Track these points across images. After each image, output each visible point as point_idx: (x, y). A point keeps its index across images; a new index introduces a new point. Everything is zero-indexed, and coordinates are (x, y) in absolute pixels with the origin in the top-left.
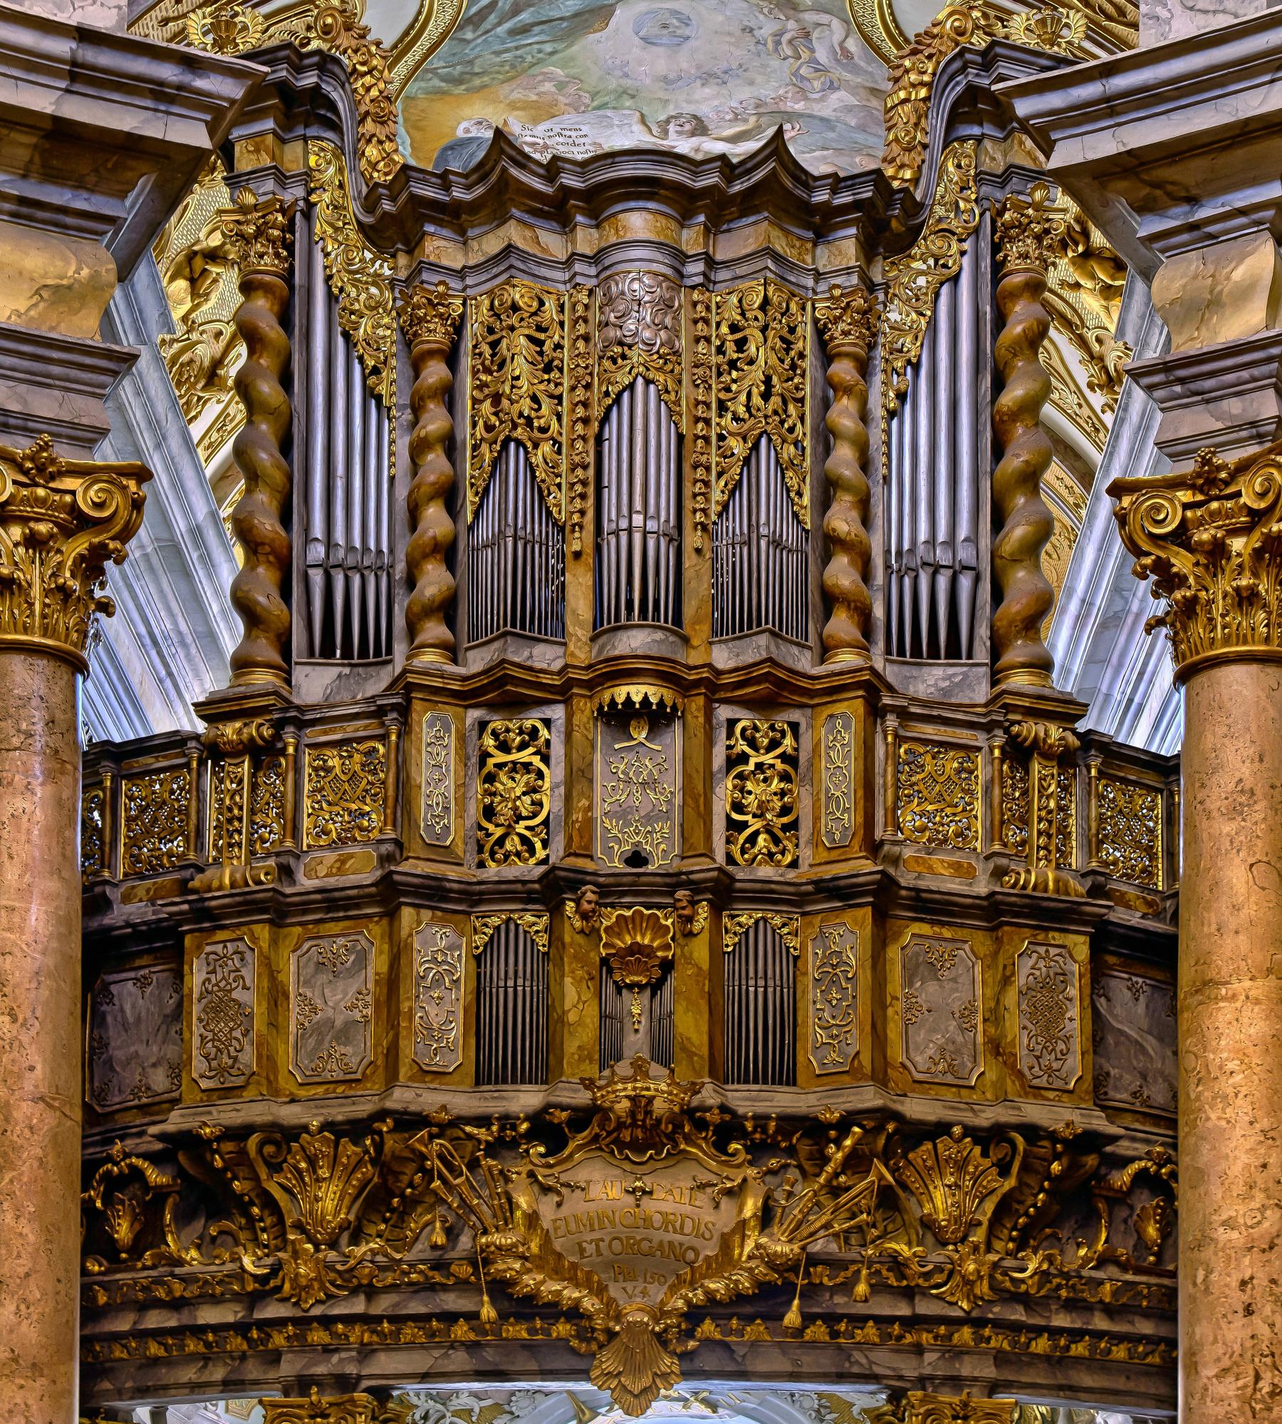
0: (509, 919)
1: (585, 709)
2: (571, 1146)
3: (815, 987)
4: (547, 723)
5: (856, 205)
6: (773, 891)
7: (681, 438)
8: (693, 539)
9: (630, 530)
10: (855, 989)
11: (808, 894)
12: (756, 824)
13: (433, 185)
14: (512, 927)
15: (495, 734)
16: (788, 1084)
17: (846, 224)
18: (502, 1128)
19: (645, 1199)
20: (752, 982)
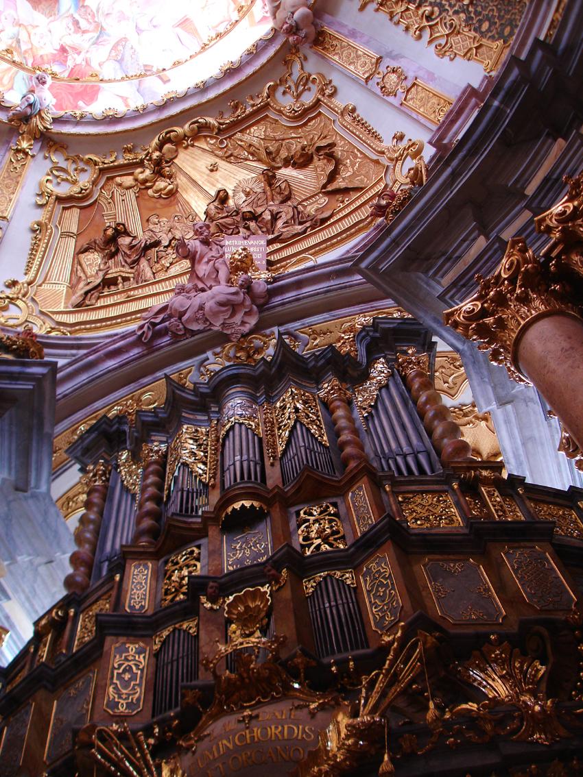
0: (175, 629)
1: (213, 531)
2: (204, 719)
3: (369, 596)
4: (199, 547)
5: (328, 362)
6: (330, 558)
7: (260, 440)
8: (267, 463)
9: (234, 464)
10: (391, 580)
11: (353, 554)
12: (319, 541)
13: (151, 416)
14: (177, 632)
15: (172, 561)
16: (363, 648)
17: (327, 372)
18: (162, 732)
19: (254, 722)
20: (327, 605)
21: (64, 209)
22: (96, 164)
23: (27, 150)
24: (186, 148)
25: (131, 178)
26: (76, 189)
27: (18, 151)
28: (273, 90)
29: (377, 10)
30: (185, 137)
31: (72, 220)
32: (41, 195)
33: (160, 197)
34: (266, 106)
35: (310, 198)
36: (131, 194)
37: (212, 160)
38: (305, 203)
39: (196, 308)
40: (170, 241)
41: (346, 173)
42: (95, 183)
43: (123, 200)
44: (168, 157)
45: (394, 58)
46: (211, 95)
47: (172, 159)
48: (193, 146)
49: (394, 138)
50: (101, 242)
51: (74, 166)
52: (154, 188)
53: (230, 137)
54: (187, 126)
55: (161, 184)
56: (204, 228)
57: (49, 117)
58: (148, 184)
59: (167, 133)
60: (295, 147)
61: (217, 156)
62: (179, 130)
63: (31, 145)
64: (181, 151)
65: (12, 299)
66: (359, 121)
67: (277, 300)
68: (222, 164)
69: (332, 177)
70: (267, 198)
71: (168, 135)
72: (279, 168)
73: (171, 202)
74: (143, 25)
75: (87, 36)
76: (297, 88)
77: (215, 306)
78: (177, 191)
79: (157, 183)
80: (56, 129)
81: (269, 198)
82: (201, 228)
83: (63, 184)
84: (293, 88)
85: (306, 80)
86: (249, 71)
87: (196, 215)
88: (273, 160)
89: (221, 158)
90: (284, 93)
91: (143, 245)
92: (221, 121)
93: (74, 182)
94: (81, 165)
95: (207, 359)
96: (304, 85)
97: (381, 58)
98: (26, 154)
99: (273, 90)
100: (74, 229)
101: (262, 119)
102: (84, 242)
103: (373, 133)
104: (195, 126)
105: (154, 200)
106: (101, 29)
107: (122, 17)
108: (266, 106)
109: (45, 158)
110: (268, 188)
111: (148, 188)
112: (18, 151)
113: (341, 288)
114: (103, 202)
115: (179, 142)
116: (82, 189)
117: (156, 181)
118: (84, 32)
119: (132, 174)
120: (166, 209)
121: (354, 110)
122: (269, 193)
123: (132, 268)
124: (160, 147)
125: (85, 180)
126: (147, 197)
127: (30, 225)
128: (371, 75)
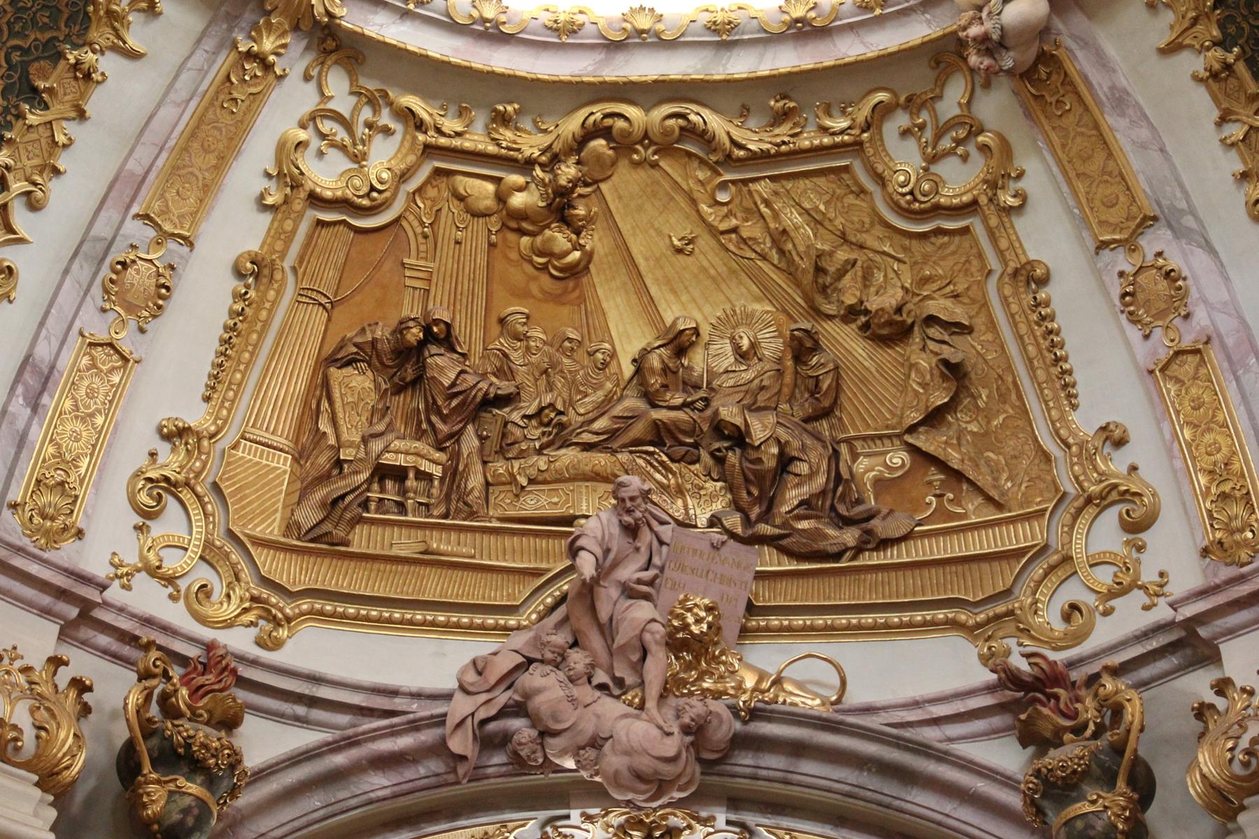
22: (420, 126)
23: (272, 58)
25: (490, 187)
28: (882, 112)
29: (1197, 78)
33: (544, 268)
35: (872, 438)
38: (858, 444)
39: (583, 740)
40: (541, 410)
41: (965, 421)
43: (457, 242)
45: (1179, 232)
46: (740, 65)
47: (596, 182)
48: (654, 165)
49: (1103, 429)
50: (386, 347)
51: (366, 113)
52: (539, 239)
53: (745, 182)
55: (559, 238)
56: (639, 500)
58: (525, 225)
59: (606, 116)
60: (883, 300)
63: (284, 46)
64: (623, 168)
65: (176, 485)
66: (1043, 318)
67: (745, 760)
68: (705, 242)
69: (934, 418)
70: (780, 391)
71: (608, 122)
73: (565, 292)
76: (938, 136)
77: (625, 772)
78: (587, 268)
79: (548, 232)
81: (786, 390)
82: (632, 499)
83: (334, 155)
84: (928, 134)
87: (613, 355)
88: (824, 290)
90: (905, 133)
91: (478, 399)
92: (737, 134)
93: (358, 158)
94: (385, 119)
95: (568, 817)
97: (1155, 219)
98: (267, 67)
99: (882, 112)
102: (346, 327)
103: (1064, 372)
104: (672, 122)
105: (529, 269)
108: (857, 147)
109: (307, 78)
110: (789, 363)
111: (523, 232)
113: (880, 804)
114: (411, 227)
116: (373, 189)
117: (548, 226)
119: (497, 181)
120: (550, 308)
121: (1043, 281)
122: (788, 379)
123: (442, 450)
125: (383, 158)
126: (514, 255)
128: (1115, 241)
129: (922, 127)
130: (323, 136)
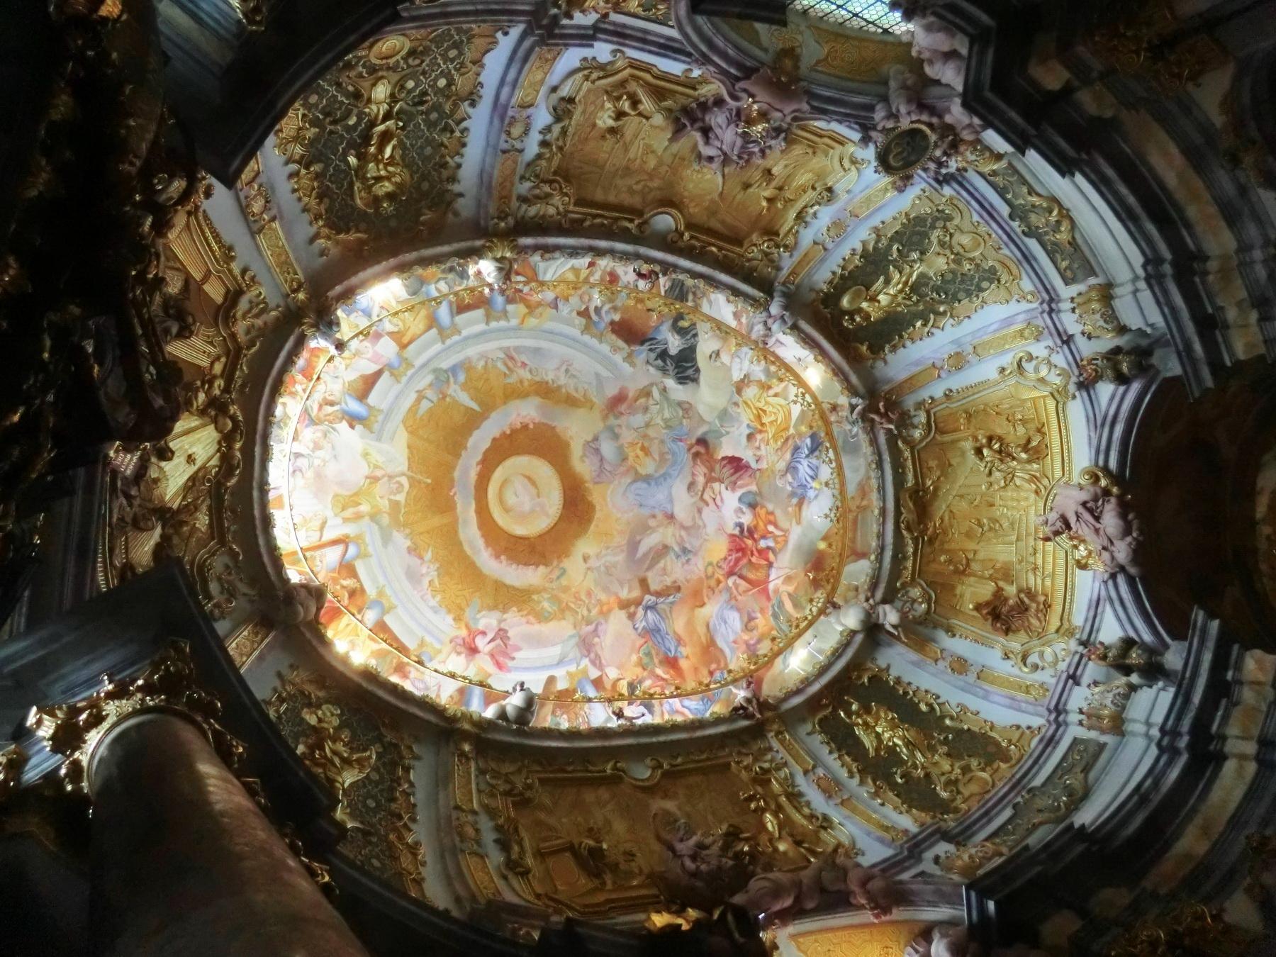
21: (228, 291)
22: (249, 348)
24: (219, 443)
26: (239, 314)
27: (300, 286)
28: (234, 555)
29: (275, 690)
30: (230, 447)
31: (215, 291)
32: (253, 279)
34: (222, 542)
36: (204, 362)
37: (199, 463)
42: (233, 336)
44: (221, 419)
48: (218, 450)
54: (238, 454)
57: (309, 332)
61: (200, 469)
62: (238, 445)
68: (192, 470)
72: (163, 528)
74: (302, 462)
75: (316, 407)
80: (297, 331)
85: (231, 594)
86: (261, 541)
88: (172, 526)
89: (197, 472)
94: (254, 333)
96: (228, 590)
99: (234, 555)
100: (206, 287)
101: (212, 533)
102: (193, 287)
106: (313, 422)
107: (317, 447)
108: (222, 542)
109: (278, 306)
112: (300, 286)
115: (227, 439)
118: (320, 407)
124: (233, 418)
127: (237, 249)
129: (230, 574)
130: (258, 304)
